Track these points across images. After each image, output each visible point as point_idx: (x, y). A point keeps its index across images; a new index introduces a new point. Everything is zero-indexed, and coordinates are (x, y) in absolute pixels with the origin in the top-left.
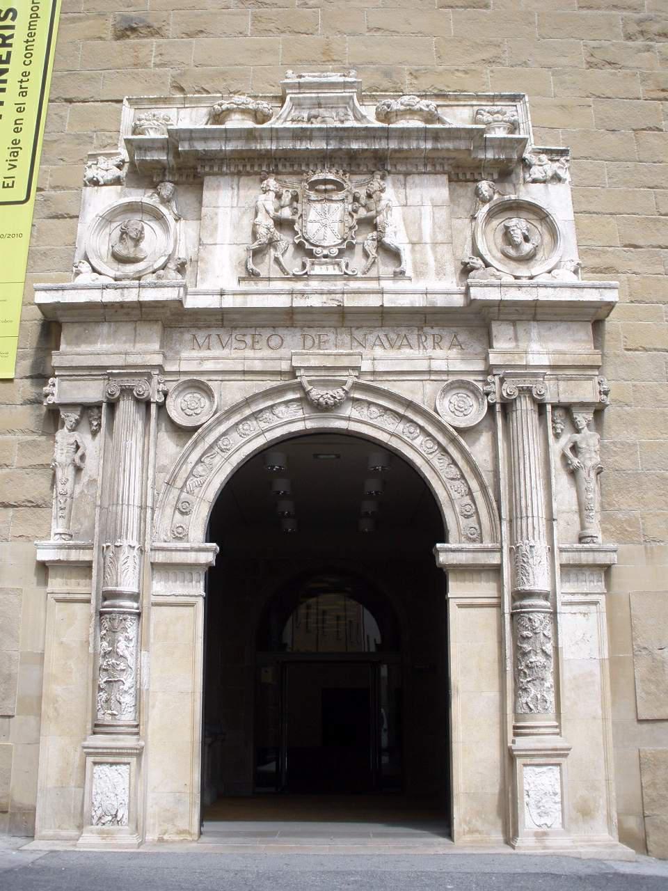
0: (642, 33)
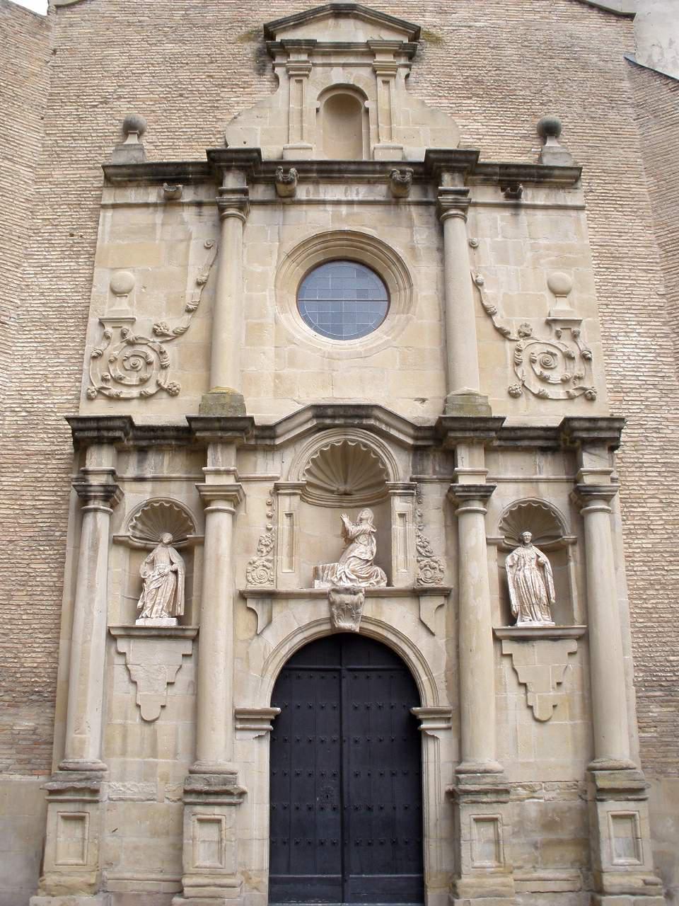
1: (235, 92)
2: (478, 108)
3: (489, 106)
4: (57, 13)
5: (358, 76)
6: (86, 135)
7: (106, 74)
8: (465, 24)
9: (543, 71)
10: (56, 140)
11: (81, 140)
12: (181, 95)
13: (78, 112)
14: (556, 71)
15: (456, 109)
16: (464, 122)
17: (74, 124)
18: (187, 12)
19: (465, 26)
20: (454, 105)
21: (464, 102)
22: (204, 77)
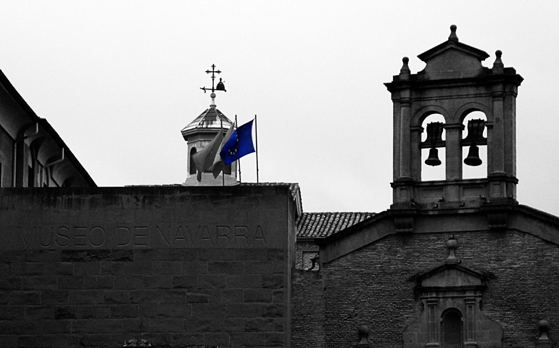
0: (269, 314)
1: (406, 311)
2: (513, 316)
3: (518, 314)
4: (324, 267)
5: (458, 304)
6: (344, 335)
7: (349, 301)
8: (509, 267)
9: (544, 292)
10: (331, 338)
11: (342, 338)
12: (383, 314)
13: (339, 323)
14: (551, 292)
15: (503, 317)
16: (506, 325)
17: (338, 329)
18: (382, 265)
19: (509, 268)
20: (501, 315)
21: (507, 313)
22: (392, 303)
